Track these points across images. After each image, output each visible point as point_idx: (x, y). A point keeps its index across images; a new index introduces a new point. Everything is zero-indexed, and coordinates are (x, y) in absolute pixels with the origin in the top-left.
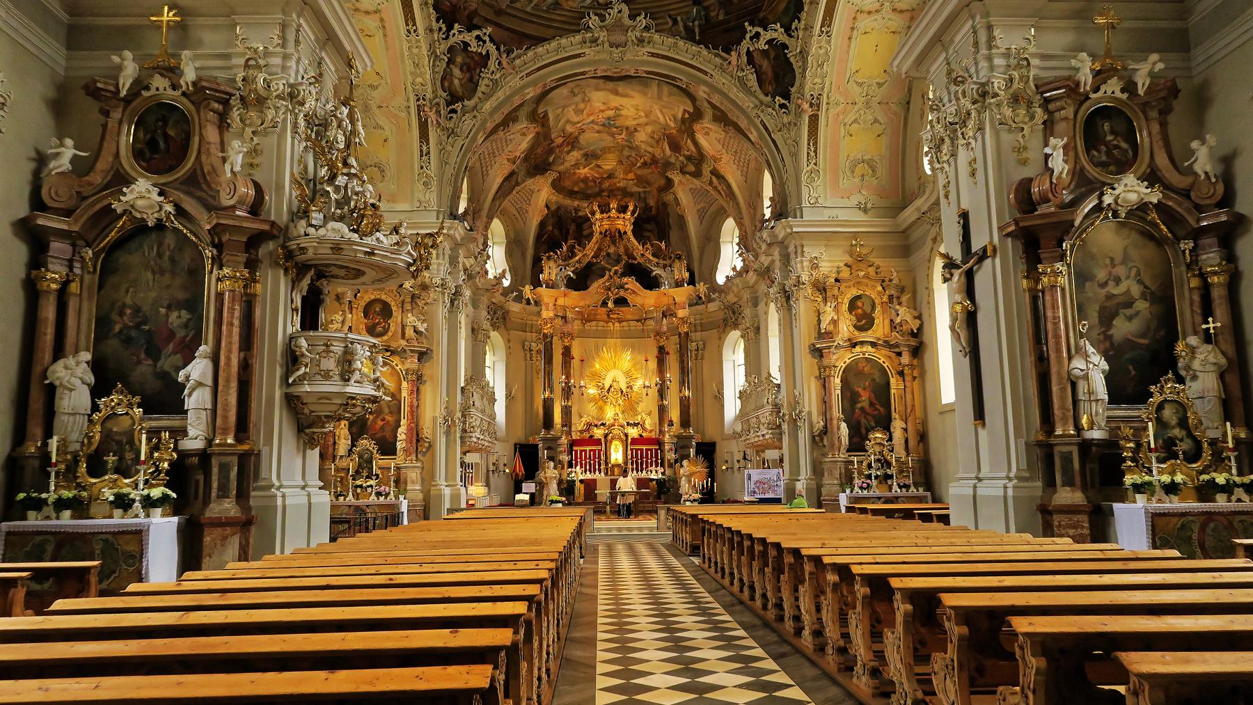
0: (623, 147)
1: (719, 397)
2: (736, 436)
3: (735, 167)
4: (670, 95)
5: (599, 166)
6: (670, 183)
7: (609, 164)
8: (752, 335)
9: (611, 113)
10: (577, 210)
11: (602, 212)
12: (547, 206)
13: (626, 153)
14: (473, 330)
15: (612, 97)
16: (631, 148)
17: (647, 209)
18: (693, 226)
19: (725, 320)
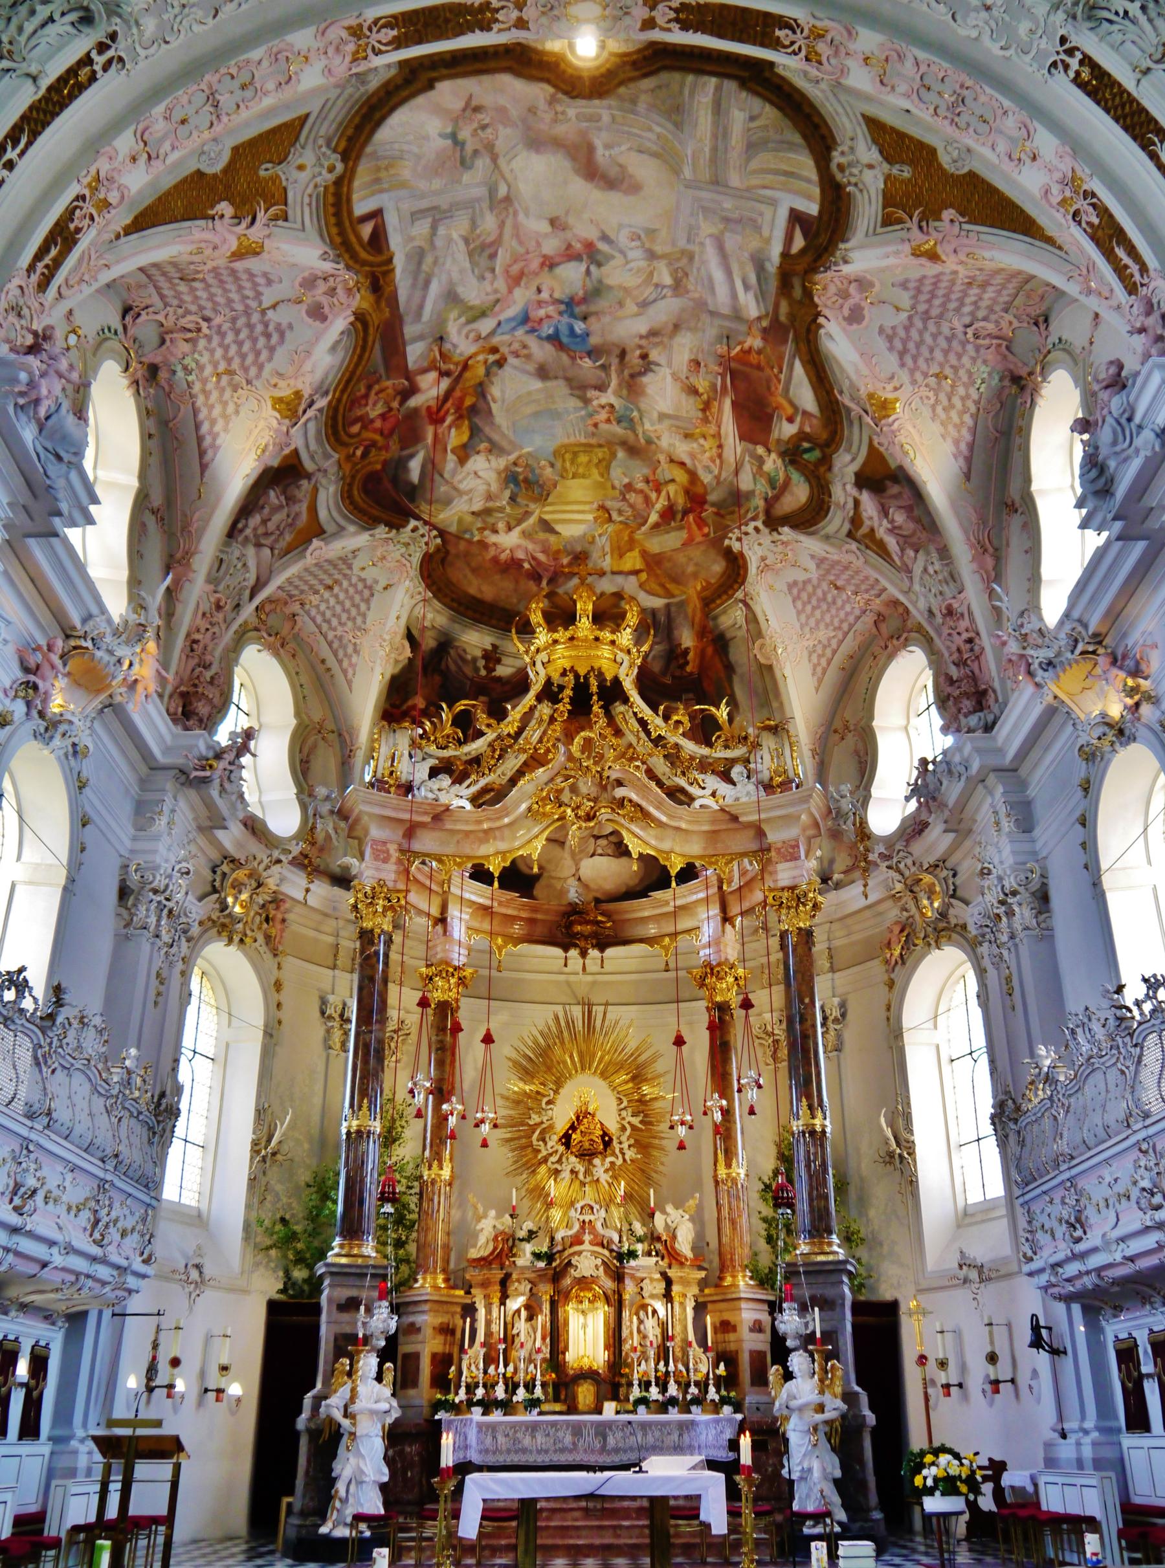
0: (611, 444)
1: (899, 1158)
2: (976, 1274)
3: (936, 428)
4: (752, 148)
5: (546, 526)
6: (736, 567)
7: (575, 516)
8: (1024, 914)
9: (572, 276)
10: (492, 657)
11: (552, 629)
12: (410, 636)
13: (618, 476)
14: (124, 893)
15: (579, 187)
16: (633, 451)
17: (674, 655)
18: (802, 697)
19: (906, 929)
